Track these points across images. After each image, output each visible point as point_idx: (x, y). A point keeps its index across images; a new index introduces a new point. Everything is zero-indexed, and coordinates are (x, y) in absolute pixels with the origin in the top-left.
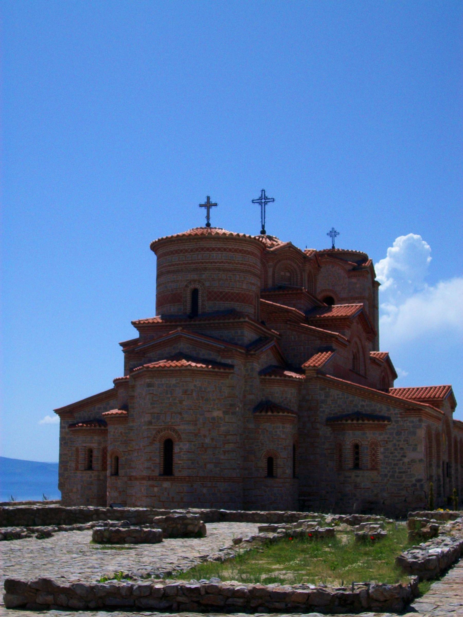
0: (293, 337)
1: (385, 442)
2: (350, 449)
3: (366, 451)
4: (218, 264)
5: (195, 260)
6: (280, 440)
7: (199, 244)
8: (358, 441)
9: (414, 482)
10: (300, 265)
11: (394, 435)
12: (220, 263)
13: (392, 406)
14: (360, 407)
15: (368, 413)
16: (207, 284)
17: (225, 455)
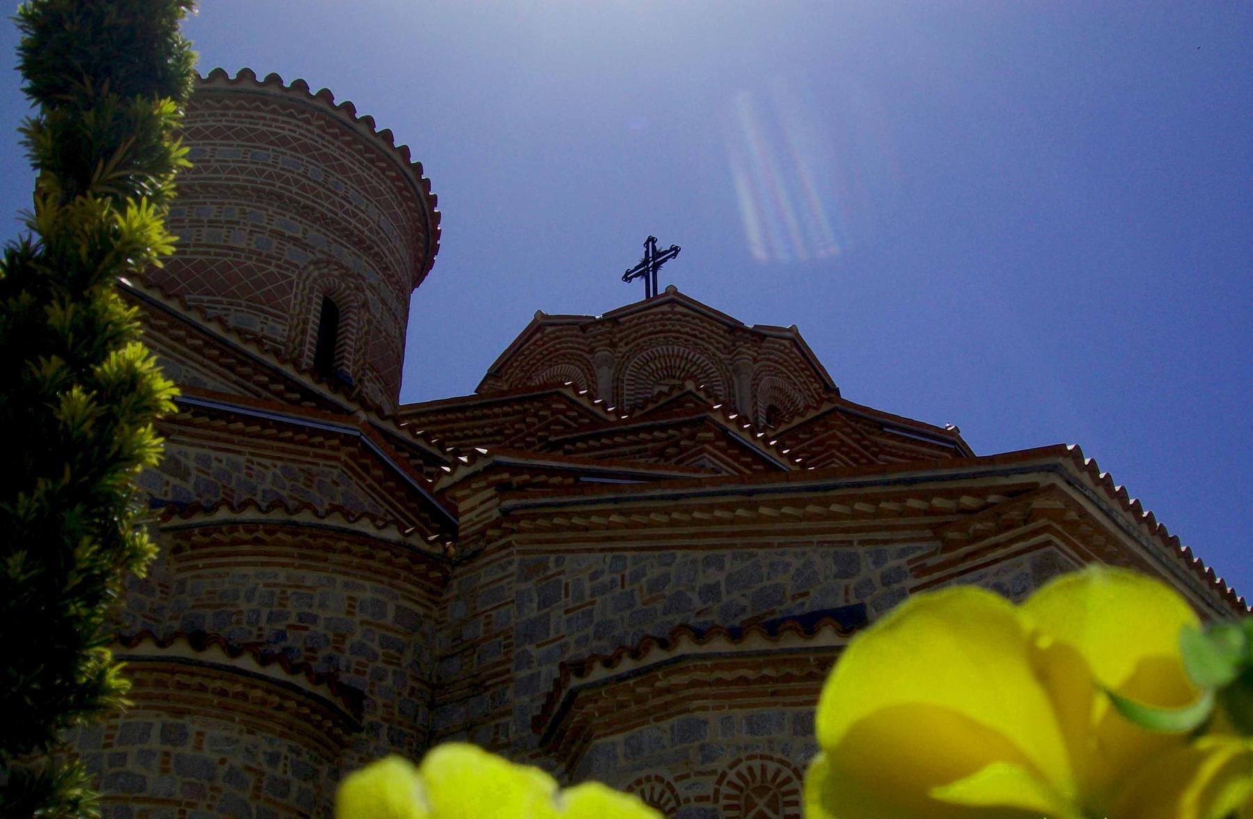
10: (723, 356)
13: (863, 543)
14: (697, 603)
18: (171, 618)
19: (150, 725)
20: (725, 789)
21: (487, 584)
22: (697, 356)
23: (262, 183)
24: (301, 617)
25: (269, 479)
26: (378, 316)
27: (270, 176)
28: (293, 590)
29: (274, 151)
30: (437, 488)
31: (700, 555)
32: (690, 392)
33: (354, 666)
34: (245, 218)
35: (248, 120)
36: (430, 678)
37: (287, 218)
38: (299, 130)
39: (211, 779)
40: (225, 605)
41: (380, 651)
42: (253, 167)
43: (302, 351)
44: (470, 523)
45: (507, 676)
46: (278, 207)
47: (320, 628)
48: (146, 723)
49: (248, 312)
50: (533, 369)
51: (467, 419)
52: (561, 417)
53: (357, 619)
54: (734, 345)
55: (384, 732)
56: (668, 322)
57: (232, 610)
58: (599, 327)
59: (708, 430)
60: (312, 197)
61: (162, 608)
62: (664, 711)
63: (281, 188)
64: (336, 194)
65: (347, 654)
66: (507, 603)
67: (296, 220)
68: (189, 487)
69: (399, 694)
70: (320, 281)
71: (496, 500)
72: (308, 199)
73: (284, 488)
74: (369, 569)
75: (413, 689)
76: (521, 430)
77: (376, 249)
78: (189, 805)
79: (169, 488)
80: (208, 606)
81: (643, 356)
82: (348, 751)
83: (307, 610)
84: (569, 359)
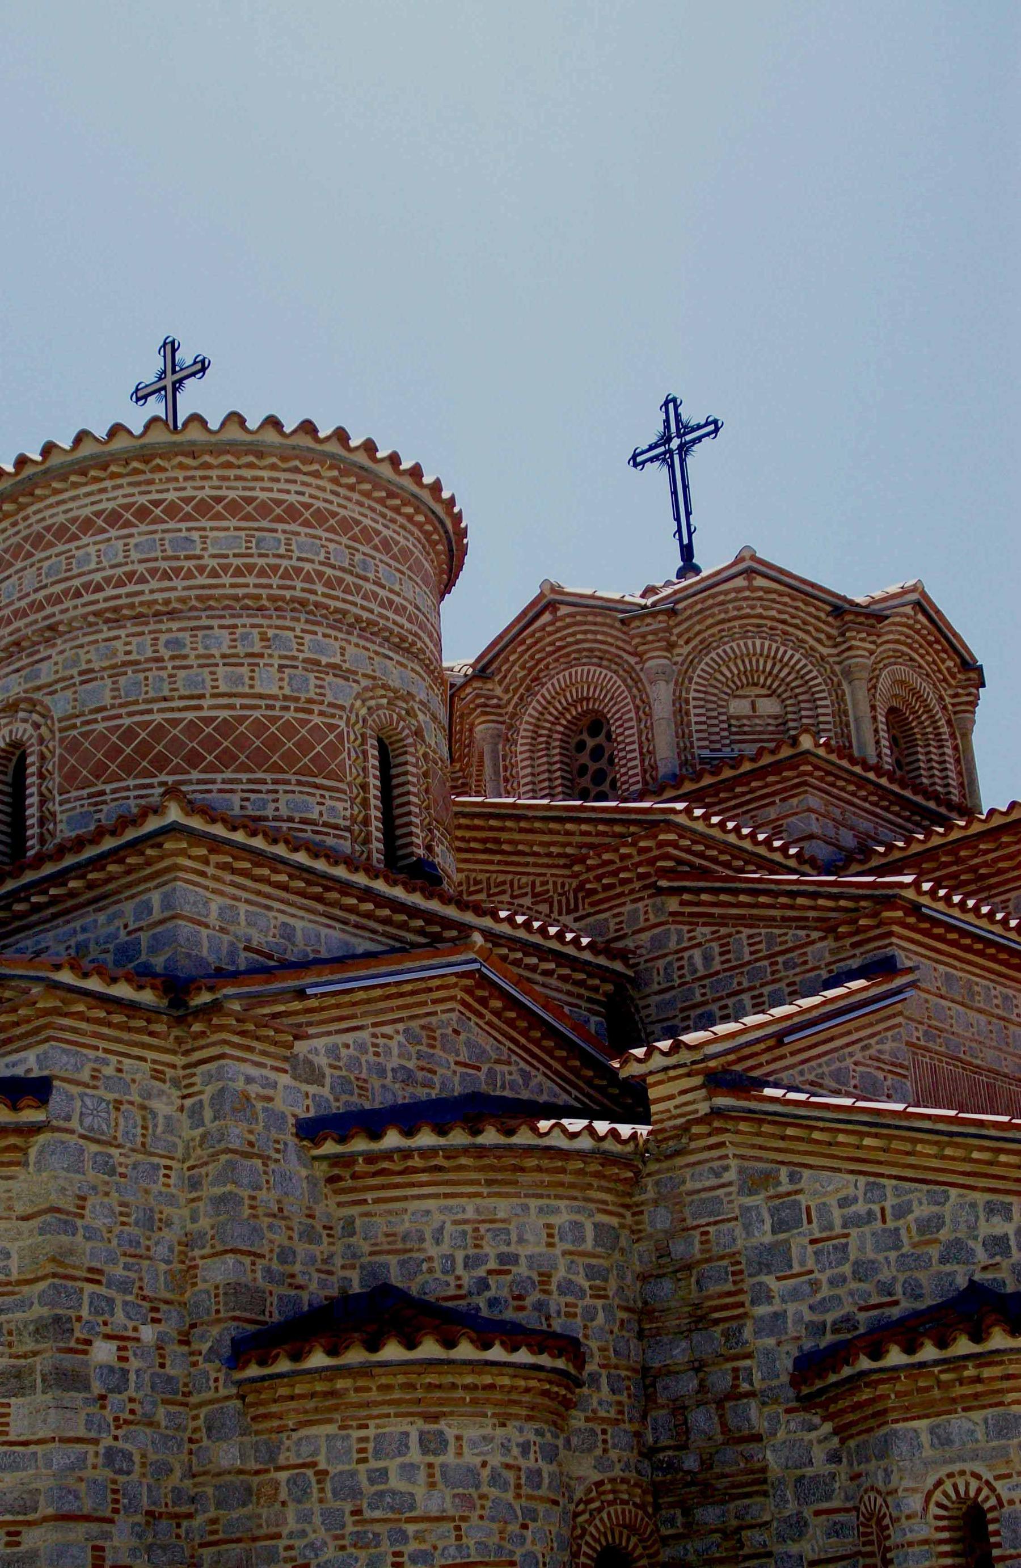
0: (697, 953)
2: (926, 1542)
5: (12, 603)
6: (411, 1528)
7: (25, 519)
10: (825, 651)
12: (120, 584)
14: (982, 1256)
16: (60, 705)
18: (343, 1267)
19: (407, 1434)
21: (699, 1191)
22: (790, 653)
23: (280, 587)
24: (502, 1258)
25: (395, 1051)
26: (433, 744)
27: (286, 575)
28: (488, 1226)
29: (284, 532)
30: (623, 1074)
31: (980, 1198)
32: (807, 752)
33: (564, 1309)
34: (269, 647)
35: (240, 484)
36: (635, 1302)
37: (320, 637)
38: (308, 490)
39: (477, 1487)
40: (411, 1250)
41: (586, 1285)
42: (261, 562)
43: (369, 834)
44: (668, 1115)
45: (741, 1310)
46: (307, 621)
47: (522, 1270)
48: (402, 1433)
49: (301, 792)
50: (542, 666)
51: (521, 830)
52: (670, 850)
53: (557, 1251)
54: (843, 634)
55: (604, 1380)
56: (744, 604)
57: (422, 1256)
58: (649, 620)
59: (894, 907)
60: (342, 595)
61: (331, 1256)
62: (972, 1403)
63: (303, 590)
64: (366, 579)
65: (555, 1295)
66: (729, 1220)
67: (330, 636)
68: (326, 1092)
69: (612, 1332)
70: (370, 722)
71: (703, 1092)
72: (336, 598)
73: (410, 1059)
74: (562, 1184)
75: (622, 1321)
76: (611, 862)
77: (419, 644)
78: (464, 1519)
79: (309, 1102)
80: (389, 1252)
81: (712, 659)
82: (573, 1412)
83: (504, 1249)
84: (601, 658)
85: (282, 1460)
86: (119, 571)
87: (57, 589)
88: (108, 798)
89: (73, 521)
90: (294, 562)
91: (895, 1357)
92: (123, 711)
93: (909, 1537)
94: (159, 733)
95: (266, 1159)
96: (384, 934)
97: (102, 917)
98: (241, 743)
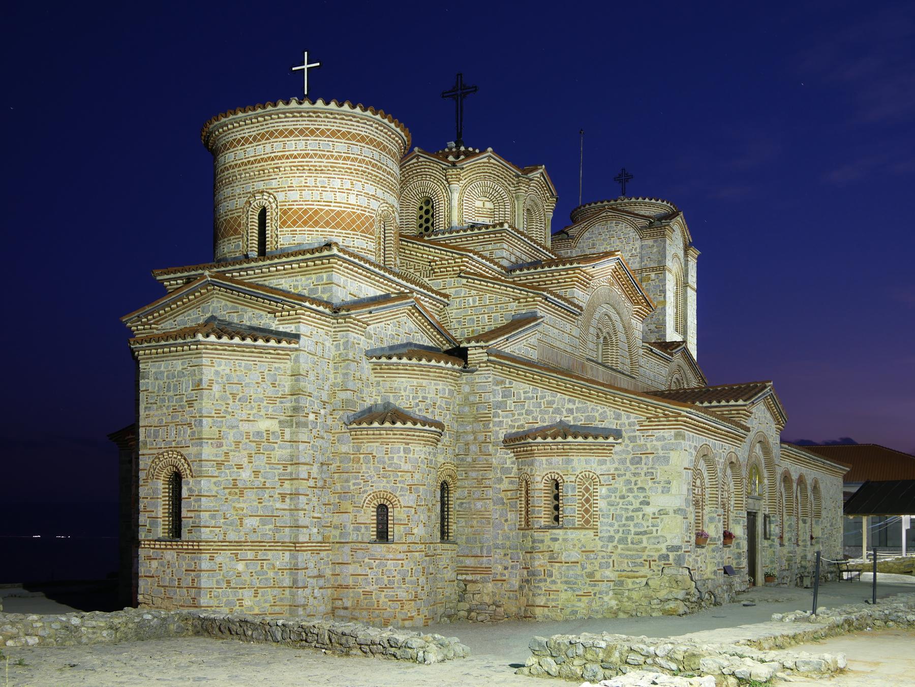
1: (611, 476)
3: (570, 494)
4: (300, 160)
6: (399, 474)
8: (557, 476)
9: (664, 551)
11: (628, 464)
14: (565, 413)
15: (579, 424)
17: (283, 501)
20: (578, 480)
24: (423, 397)
31: (567, 397)
42: (352, 156)
47: (428, 401)
85: (361, 452)
86: (303, 152)
87: (280, 154)
88: (298, 232)
89: (286, 130)
90: (363, 157)
91: (539, 440)
92: (304, 203)
93: (536, 488)
94: (316, 213)
95: (358, 363)
96: (385, 289)
97: (303, 278)
98: (343, 219)
